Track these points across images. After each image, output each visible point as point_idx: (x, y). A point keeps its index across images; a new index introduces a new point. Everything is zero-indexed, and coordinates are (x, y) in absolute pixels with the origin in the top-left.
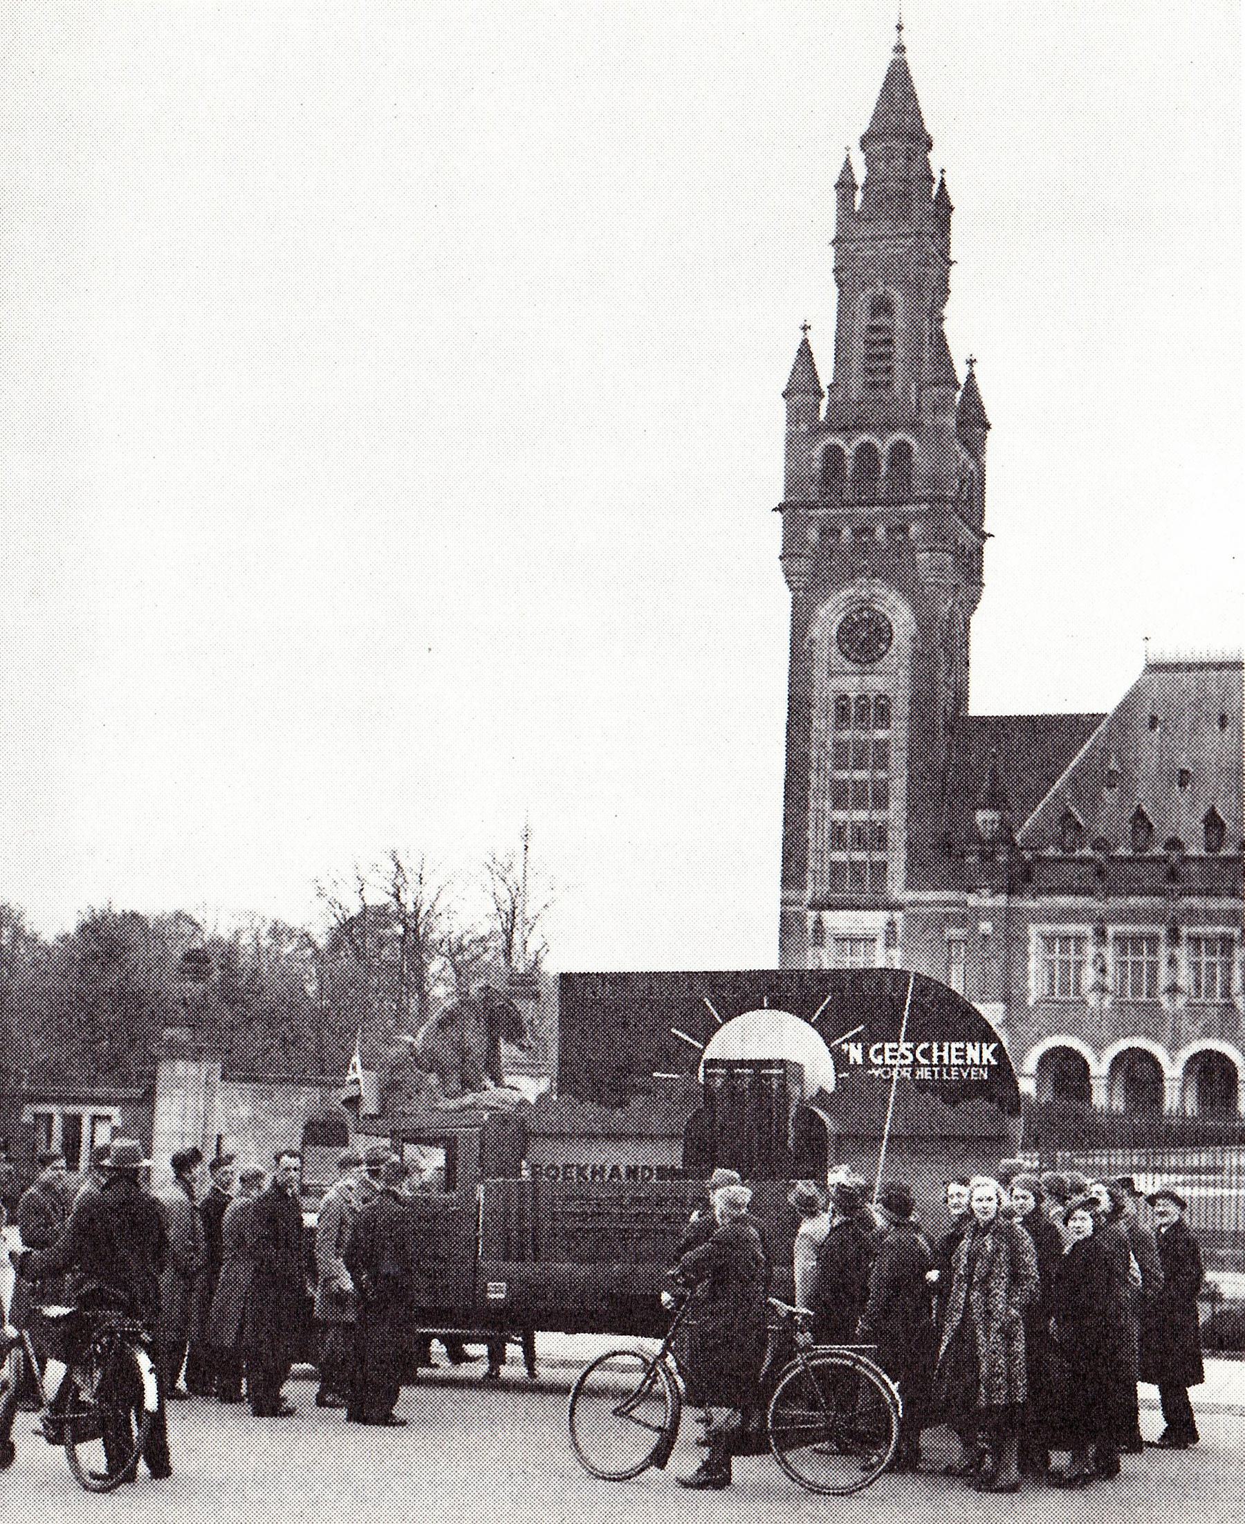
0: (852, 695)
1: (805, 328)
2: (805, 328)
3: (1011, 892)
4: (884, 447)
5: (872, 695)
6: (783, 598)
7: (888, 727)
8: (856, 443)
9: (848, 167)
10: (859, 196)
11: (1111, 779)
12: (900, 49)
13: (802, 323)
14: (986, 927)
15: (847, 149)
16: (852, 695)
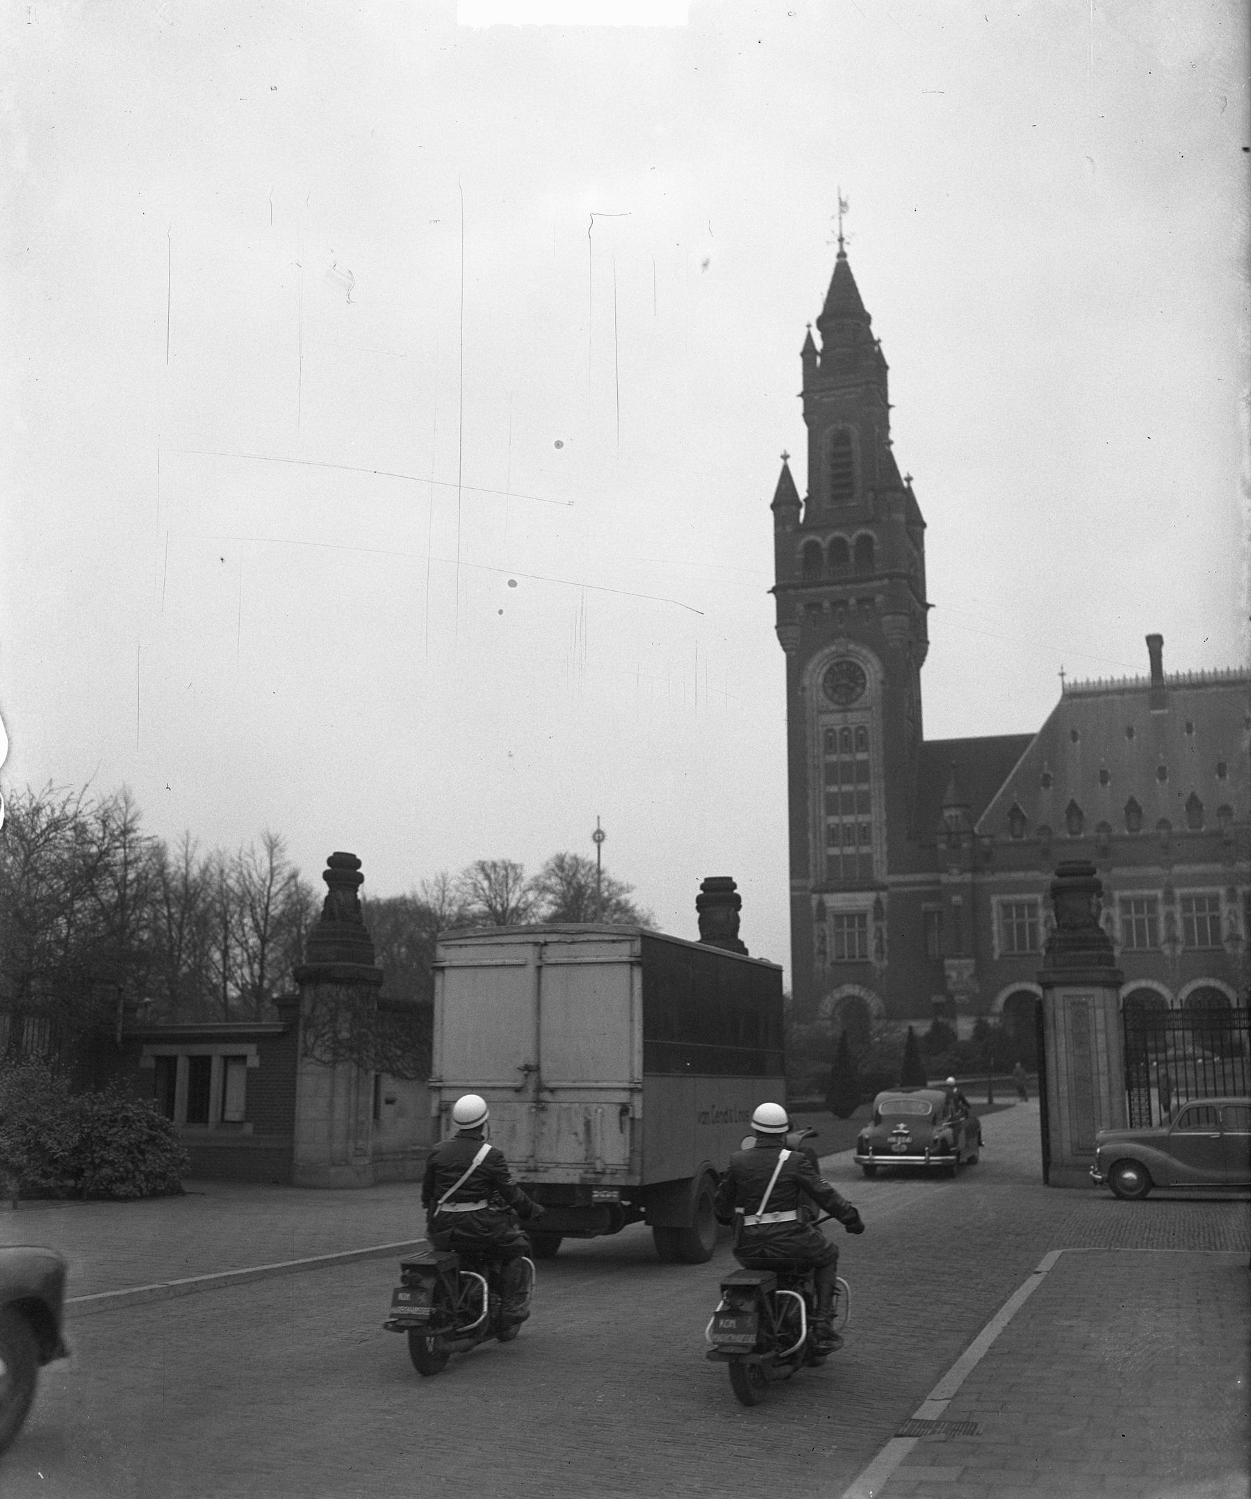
0: (838, 728)
1: (785, 457)
2: (785, 457)
3: (975, 870)
4: (851, 540)
5: (853, 727)
6: (778, 658)
7: (866, 750)
8: (829, 538)
9: (809, 339)
10: (819, 360)
11: (1046, 781)
12: (842, 255)
13: (783, 453)
14: (956, 899)
15: (809, 326)
16: (838, 728)
